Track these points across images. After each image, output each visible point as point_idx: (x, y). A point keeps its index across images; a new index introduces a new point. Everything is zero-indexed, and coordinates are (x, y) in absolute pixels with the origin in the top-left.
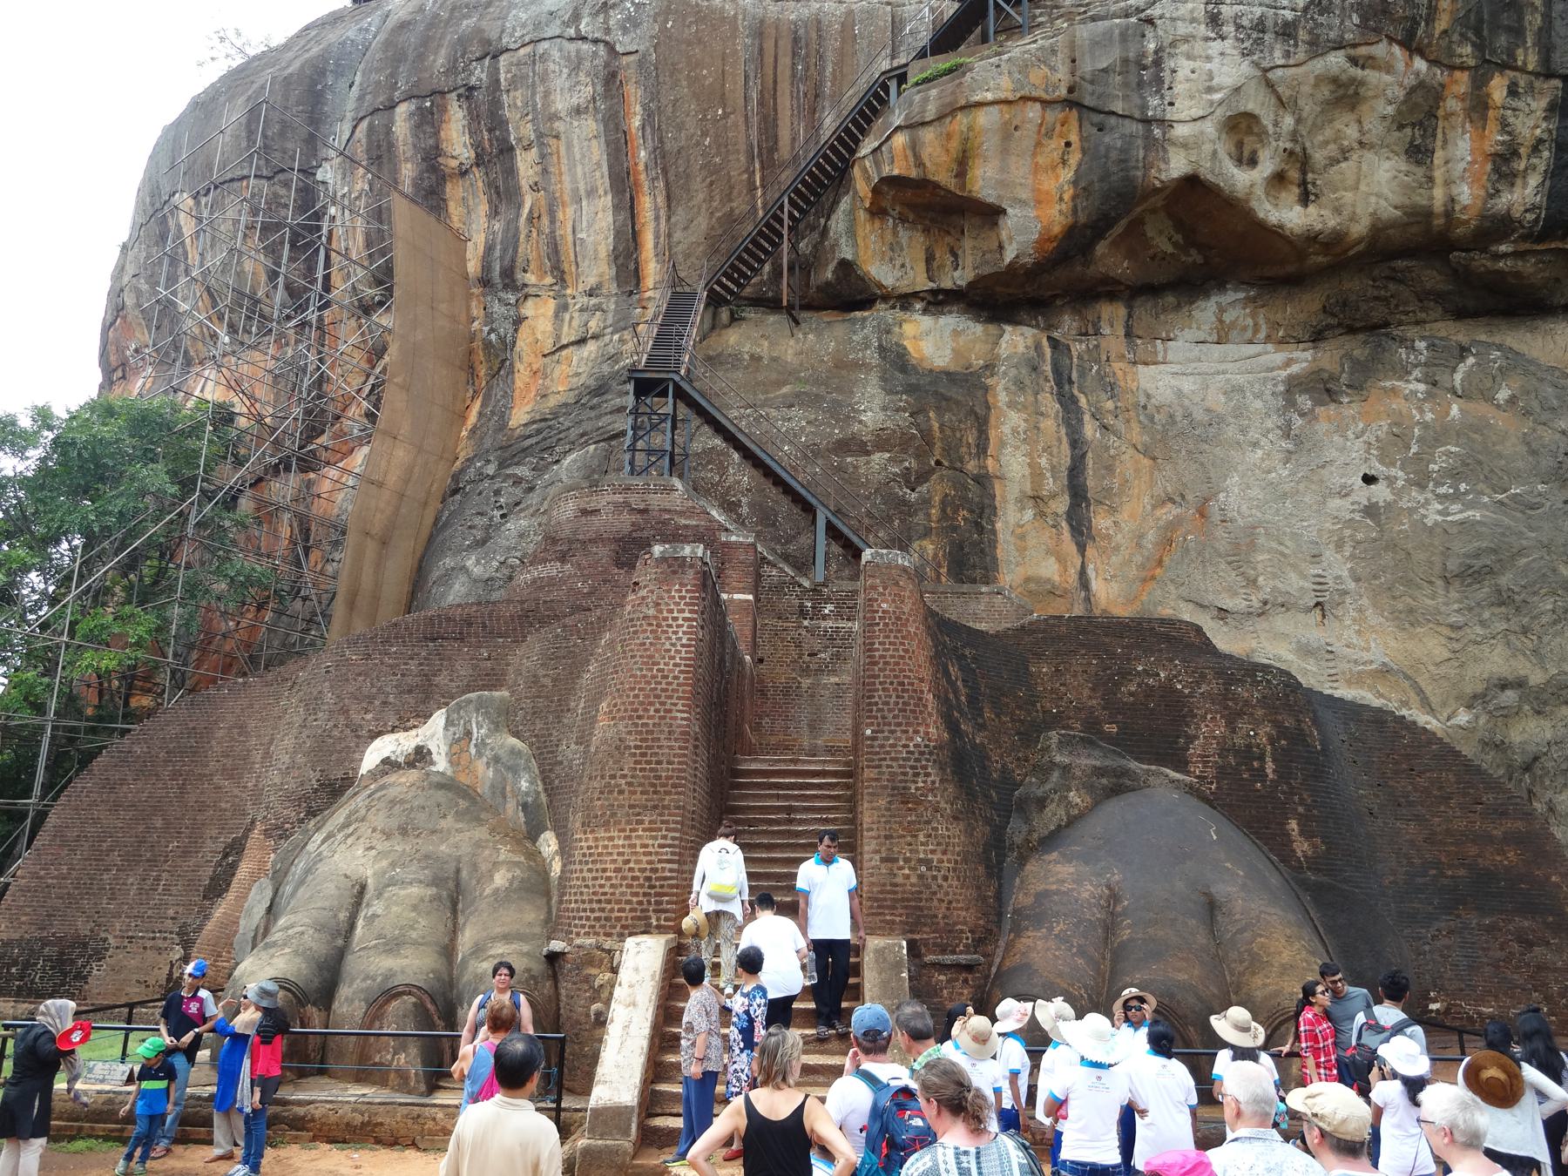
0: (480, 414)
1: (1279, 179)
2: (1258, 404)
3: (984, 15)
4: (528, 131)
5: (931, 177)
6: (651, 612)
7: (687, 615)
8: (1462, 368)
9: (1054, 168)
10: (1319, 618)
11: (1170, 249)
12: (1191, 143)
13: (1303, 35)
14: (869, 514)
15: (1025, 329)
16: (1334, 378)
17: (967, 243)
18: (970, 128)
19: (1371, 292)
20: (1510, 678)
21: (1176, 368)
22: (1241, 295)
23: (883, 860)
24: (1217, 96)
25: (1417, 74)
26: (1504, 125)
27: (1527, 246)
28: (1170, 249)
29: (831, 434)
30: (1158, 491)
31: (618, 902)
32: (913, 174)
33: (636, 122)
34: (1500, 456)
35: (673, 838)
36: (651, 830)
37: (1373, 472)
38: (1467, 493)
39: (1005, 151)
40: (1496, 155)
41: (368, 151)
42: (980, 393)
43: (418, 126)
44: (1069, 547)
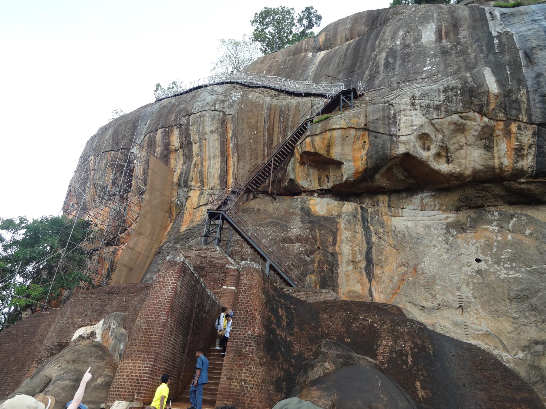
0: (172, 228)
1: (438, 155)
2: (436, 232)
3: (339, 103)
4: (197, 138)
5: (318, 152)
6: (161, 280)
7: (173, 281)
9: (360, 150)
10: (461, 312)
11: (403, 178)
12: (406, 142)
13: (443, 109)
14: (292, 264)
15: (352, 203)
17: (331, 174)
18: (331, 136)
19: (476, 195)
20: (539, 340)
21: (406, 218)
22: (429, 194)
23: (228, 379)
24: (415, 128)
25: (485, 122)
26: (518, 139)
27: (531, 180)
28: (403, 178)
29: (281, 236)
30: (399, 261)
31: (125, 388)
32: (312, 151)
33: (230, 135)
34: (528, 254)
35: (150, 364)
36: (143, 361)
37: (479, 258)
38: (516, 267)
39: (343, 144)
40: (515, 149)
41: (148, 143)
42: (335, 224)
44: (365, 280)
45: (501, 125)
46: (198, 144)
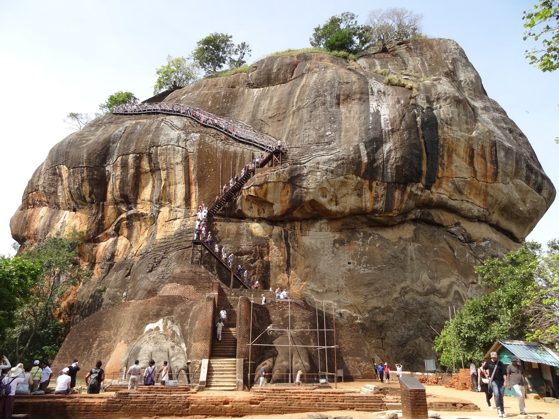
1: (331, 200)
2: (327, 246)
4: (164, 166)
8: (370, 239)
16: (344, 240)
26: (376, 192)
39: (275, 192)
43: (135, 160)
45: (367, 182)
46: (166, 171)
